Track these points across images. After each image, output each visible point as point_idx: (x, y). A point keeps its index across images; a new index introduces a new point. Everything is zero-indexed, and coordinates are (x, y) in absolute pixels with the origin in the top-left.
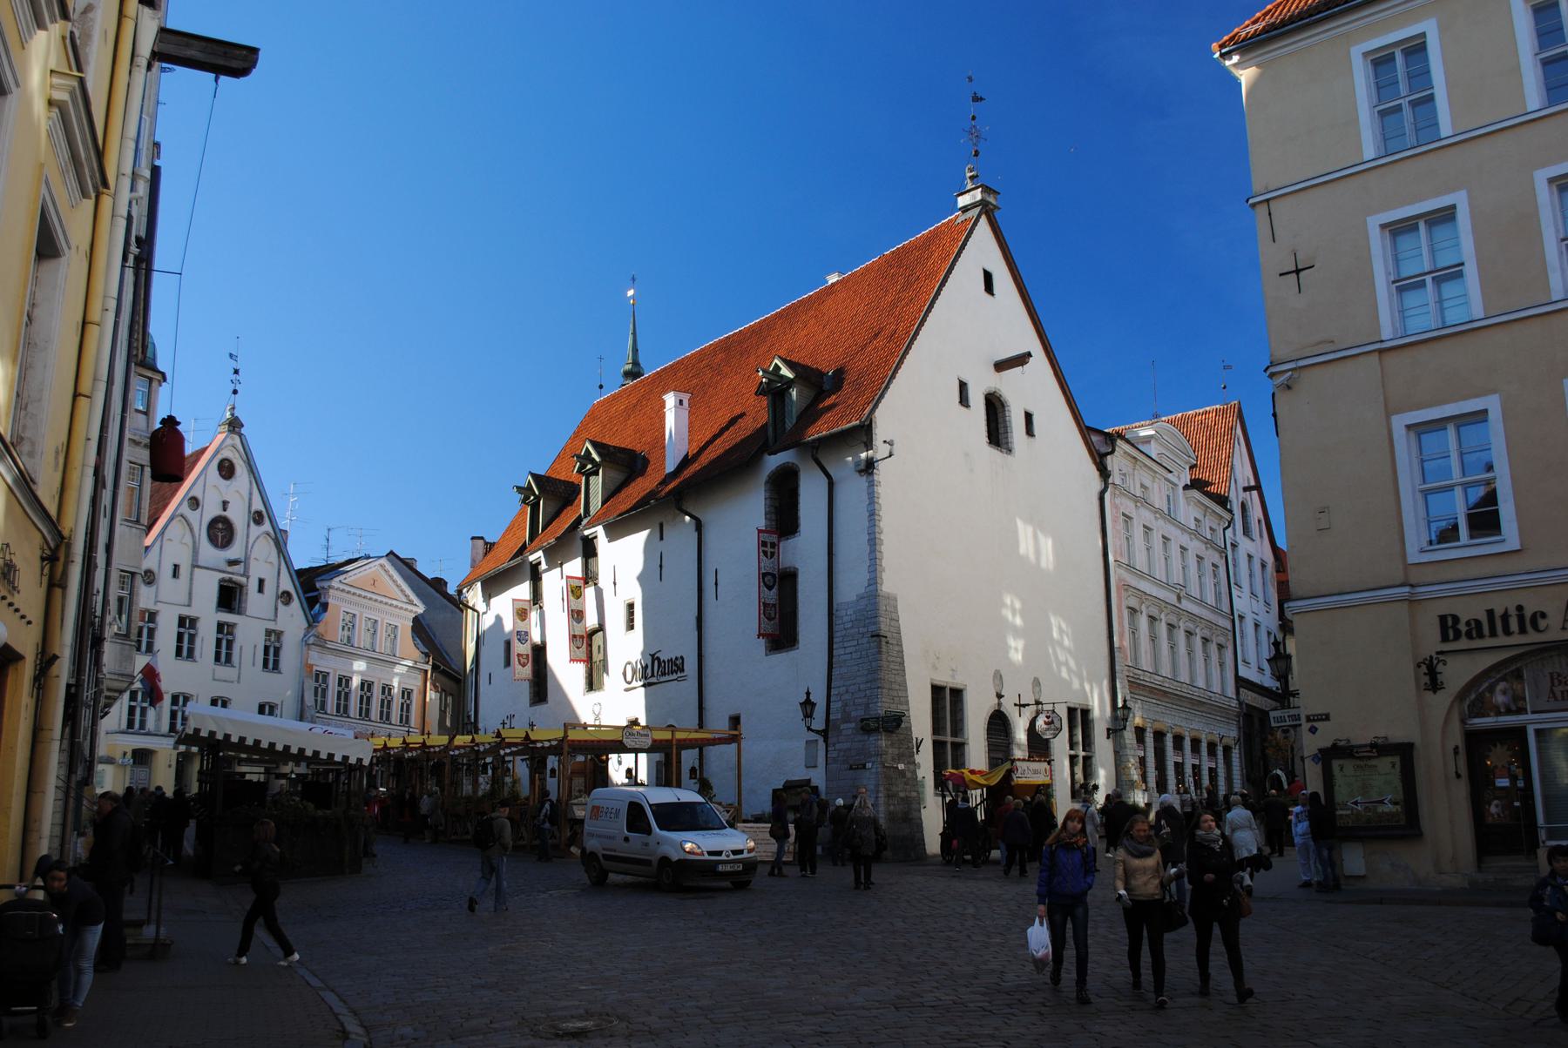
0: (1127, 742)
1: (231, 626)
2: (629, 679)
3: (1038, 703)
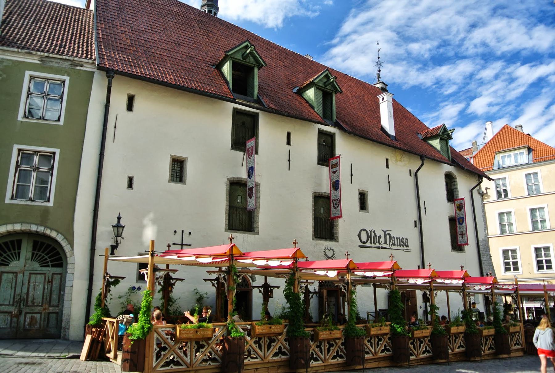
2: (364, 238)
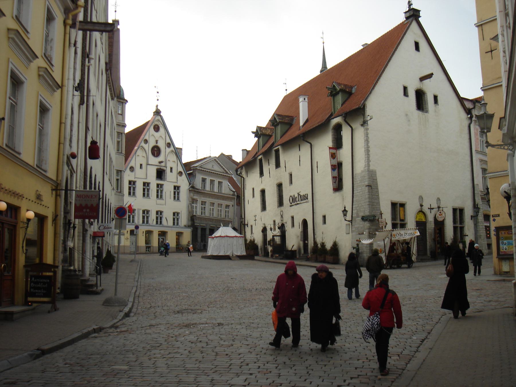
0: (479, 220)
1: (162, 185)
2: (291, 202)
3: (439, 207)
